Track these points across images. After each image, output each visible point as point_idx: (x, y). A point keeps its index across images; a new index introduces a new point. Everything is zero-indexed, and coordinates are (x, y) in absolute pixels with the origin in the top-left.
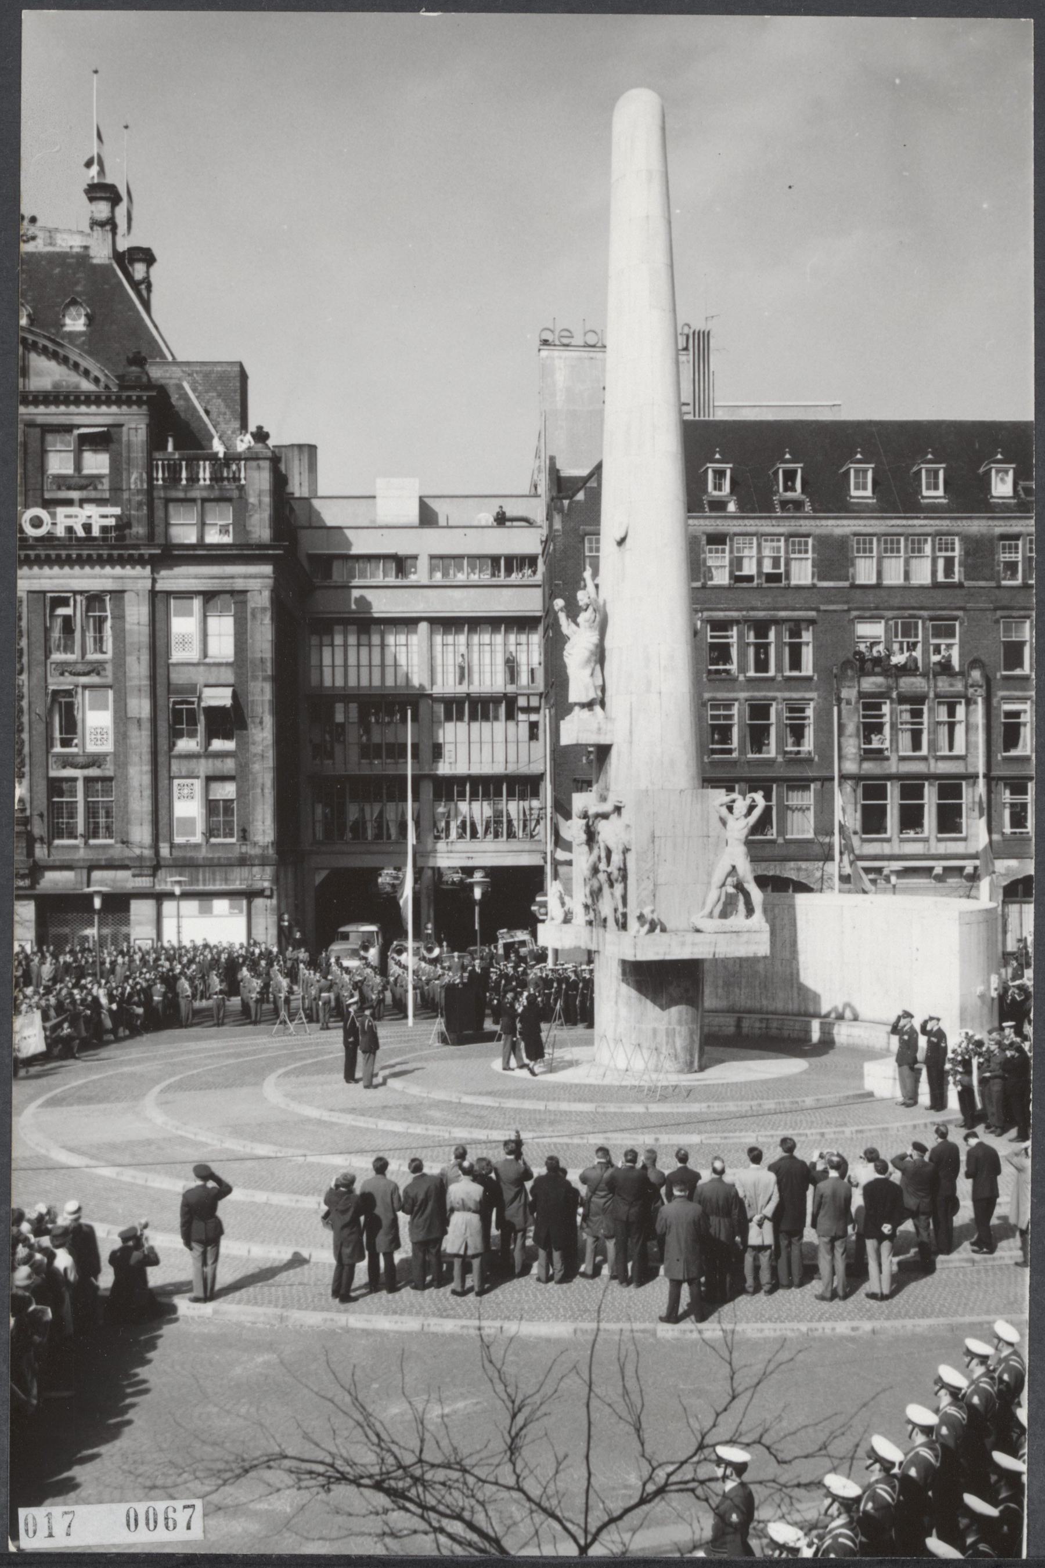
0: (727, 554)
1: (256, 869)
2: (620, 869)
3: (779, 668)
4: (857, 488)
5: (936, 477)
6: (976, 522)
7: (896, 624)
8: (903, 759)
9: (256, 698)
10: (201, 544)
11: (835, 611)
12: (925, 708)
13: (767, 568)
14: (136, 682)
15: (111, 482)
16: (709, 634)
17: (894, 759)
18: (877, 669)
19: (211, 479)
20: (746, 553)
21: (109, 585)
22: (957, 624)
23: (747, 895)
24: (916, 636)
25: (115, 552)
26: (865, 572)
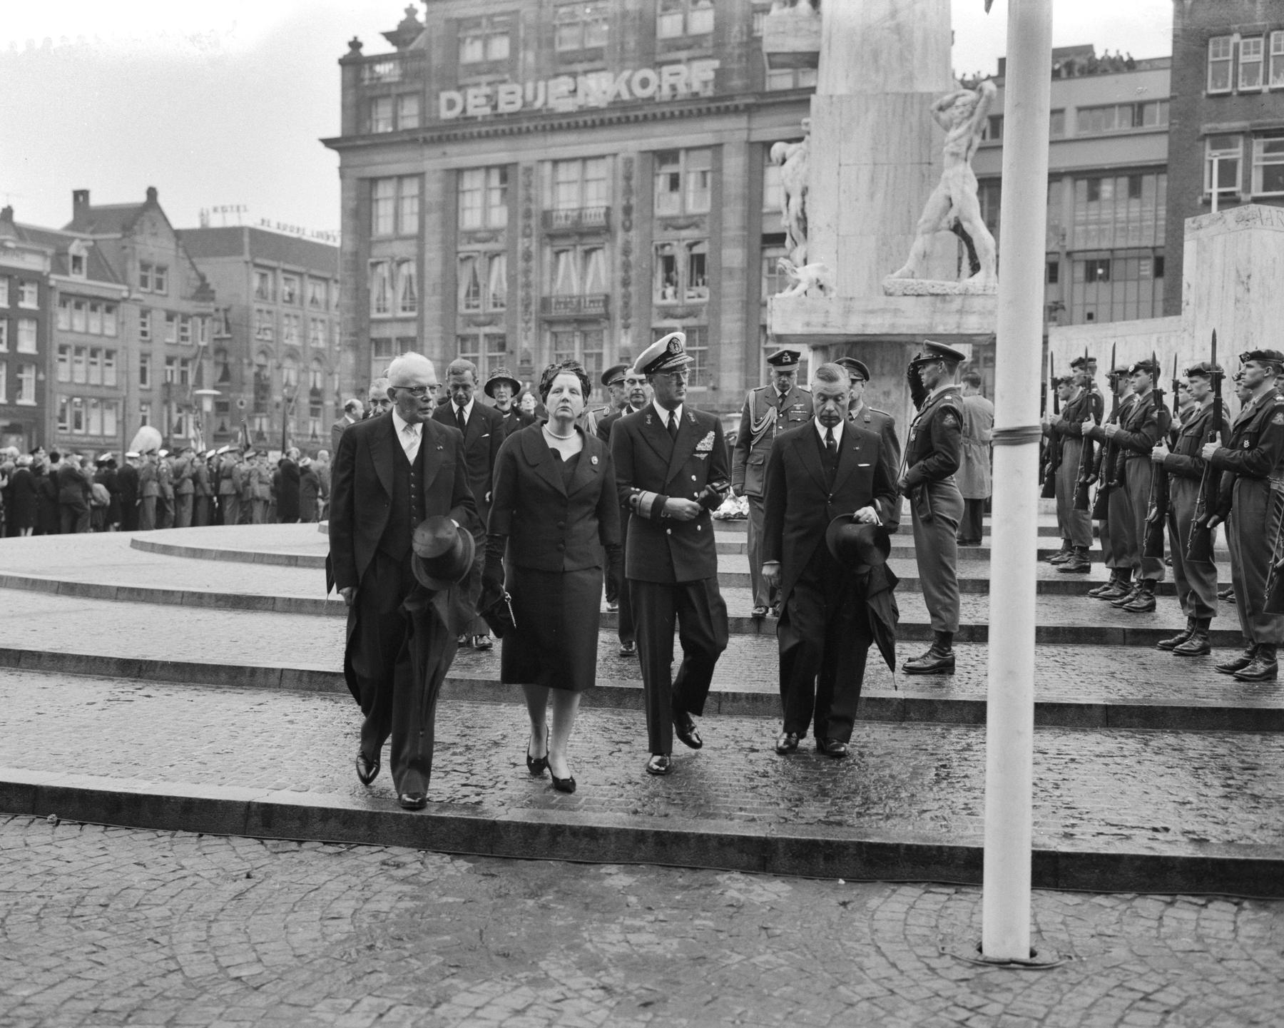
10: (795, 90)
21: (709, 139)
25: (713, 105)
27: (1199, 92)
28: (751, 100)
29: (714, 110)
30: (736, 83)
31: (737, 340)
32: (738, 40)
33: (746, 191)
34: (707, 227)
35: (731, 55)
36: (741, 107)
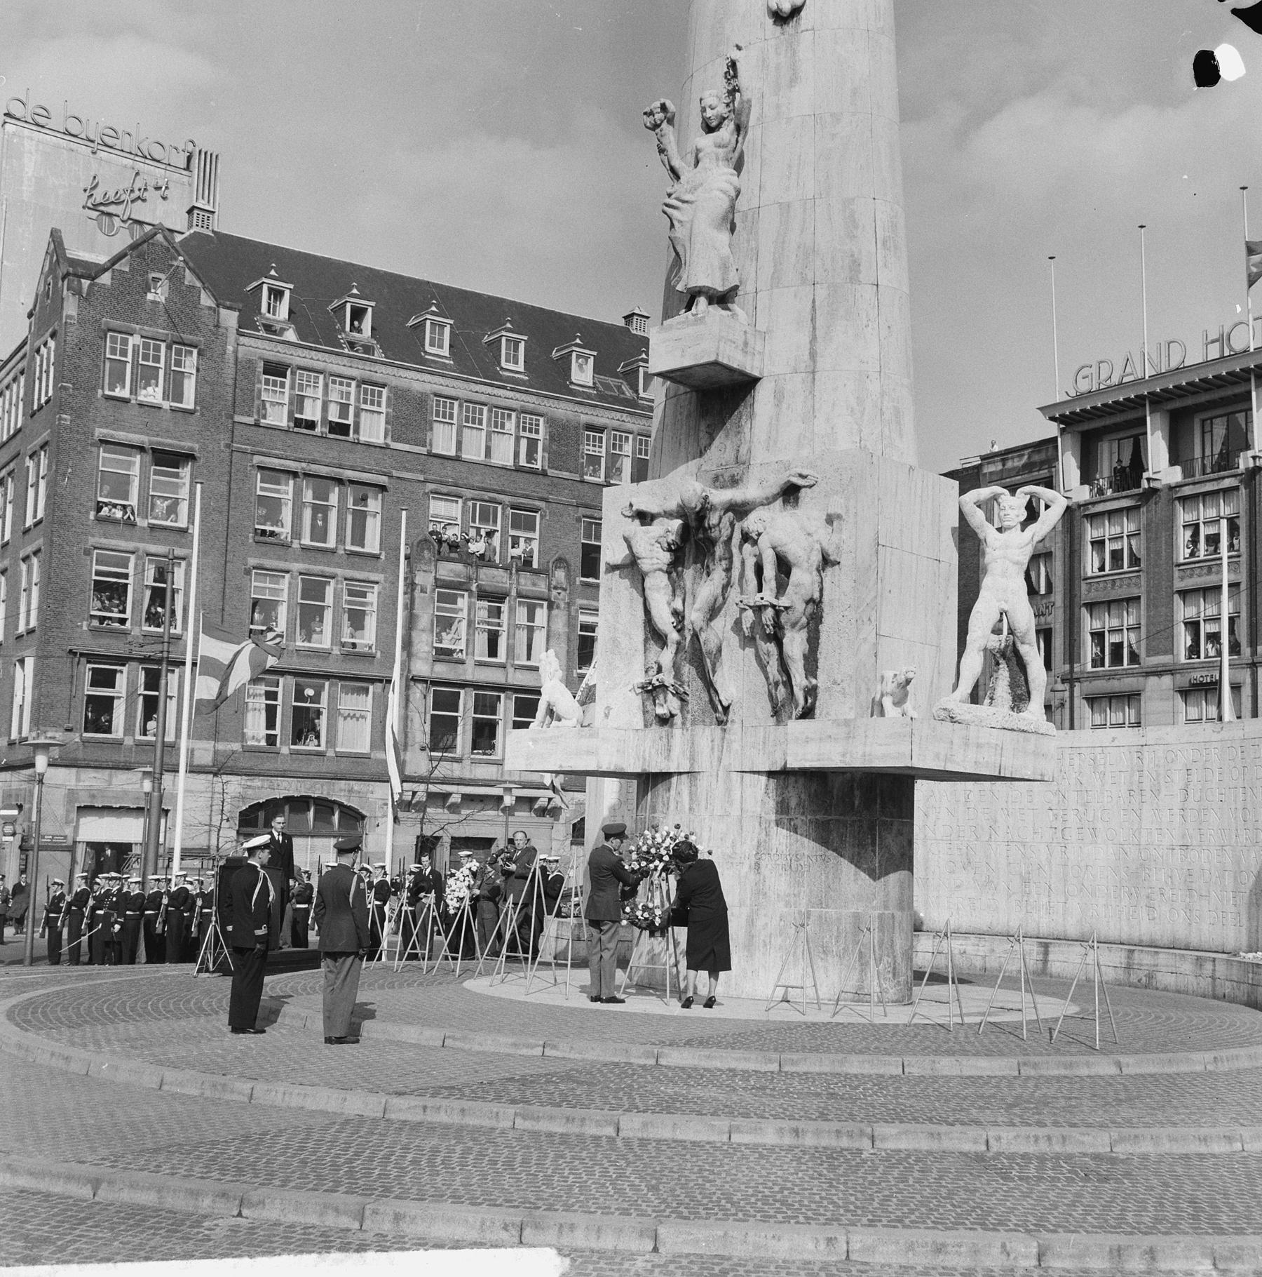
0: (287, 390)
2: (810, 601)
3: (341, 539)
4: (432, 345)
5: (516, 349)
6: (563, 405)
7: (474, 505)
8: (480, 664)
11: (409, 480)
12: (505, 607)
13: (334, 416)
16: (259, 484)
17: (470, 663)
18: (453, 555)
20: (308, 392)
22: (538, 515)
23: (1019, 664)
24: (495, 522)
26: (443, 440)
27: (94, 389)
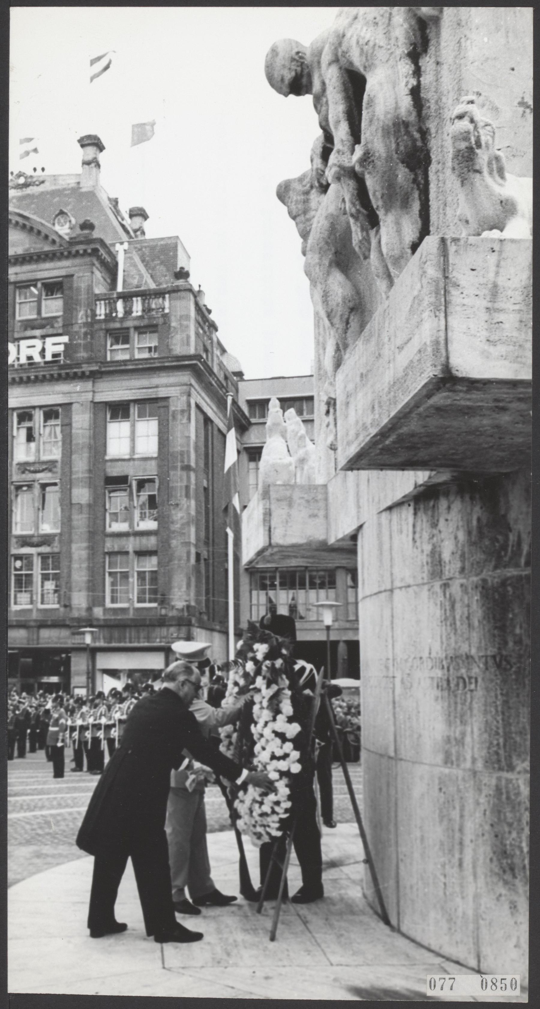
1: (172, 629)
9: (175, 484)
10: (132, 361)
14: (80, 475)
15: (64, 320)
19: (143, 311)
25: (63, 372)
28: (95, 368)
29: (63, 375)
30: (82, 354)
31: (85, 565)
32: (84, 320)
33: (92, 442)
34: (58, 469)
35: (77, 332)
36: (87, 373)
